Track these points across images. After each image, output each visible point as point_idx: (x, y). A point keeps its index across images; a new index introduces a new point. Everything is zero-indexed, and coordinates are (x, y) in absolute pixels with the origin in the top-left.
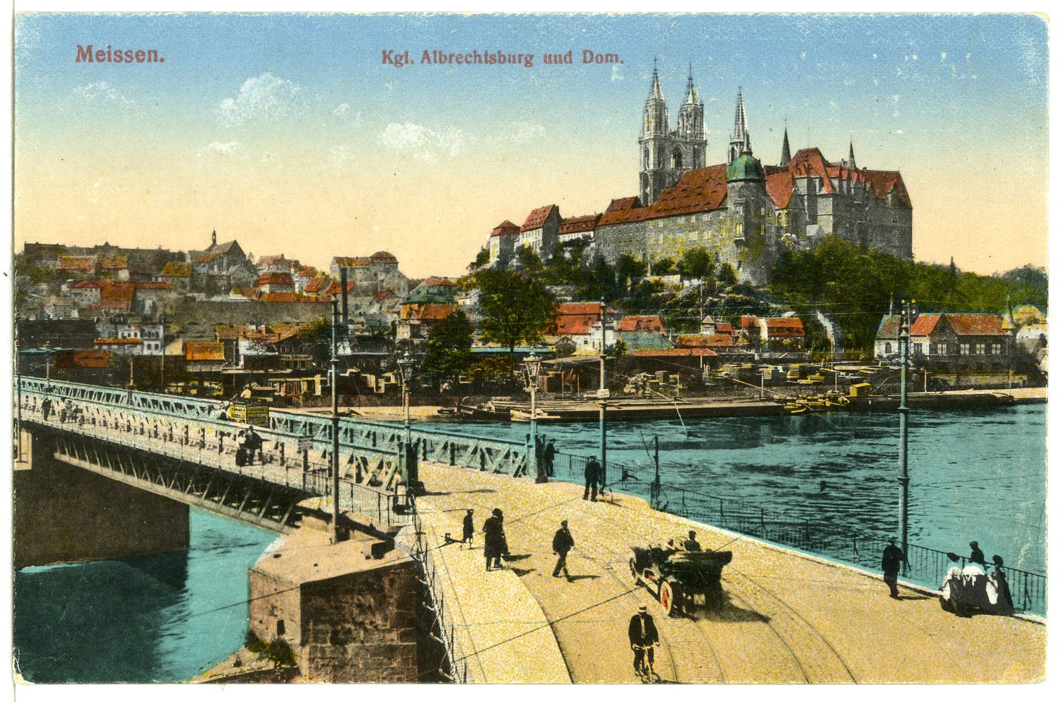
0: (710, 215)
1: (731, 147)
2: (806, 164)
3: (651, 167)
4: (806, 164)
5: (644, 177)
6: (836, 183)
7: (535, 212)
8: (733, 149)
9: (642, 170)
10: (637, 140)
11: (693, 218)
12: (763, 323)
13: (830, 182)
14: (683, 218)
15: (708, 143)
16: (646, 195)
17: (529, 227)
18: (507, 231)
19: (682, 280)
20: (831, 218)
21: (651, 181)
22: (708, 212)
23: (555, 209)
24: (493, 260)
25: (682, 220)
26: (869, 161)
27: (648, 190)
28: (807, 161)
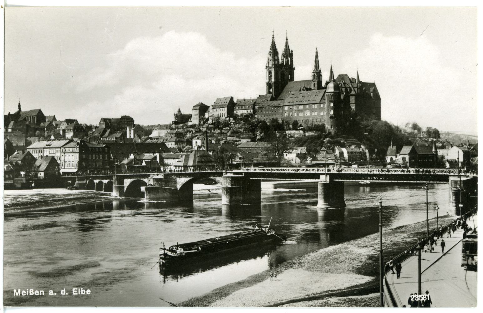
0: (315, 106)
2: (343, 81)
3: (273, 80)
4: (343, 81)
5: (269, 85)
6: (356, 89)
8: (314, 75)
9: (268, 81)
10: (265, 67)
11: (307, 106)
12: (344, 150)
13: (354, 90)
14: (302, 106)
15: (295, 69)
16: (270, 93)
17: (216, 106)
18: (203, 109)
19: (304, 133)
20: (355, 104)
22: (315, 104)
23: (232, 99)
24: (195, 121)
25: (301, 107)
26: (363, 79)
27: (271, 90)
28: (344, 80)
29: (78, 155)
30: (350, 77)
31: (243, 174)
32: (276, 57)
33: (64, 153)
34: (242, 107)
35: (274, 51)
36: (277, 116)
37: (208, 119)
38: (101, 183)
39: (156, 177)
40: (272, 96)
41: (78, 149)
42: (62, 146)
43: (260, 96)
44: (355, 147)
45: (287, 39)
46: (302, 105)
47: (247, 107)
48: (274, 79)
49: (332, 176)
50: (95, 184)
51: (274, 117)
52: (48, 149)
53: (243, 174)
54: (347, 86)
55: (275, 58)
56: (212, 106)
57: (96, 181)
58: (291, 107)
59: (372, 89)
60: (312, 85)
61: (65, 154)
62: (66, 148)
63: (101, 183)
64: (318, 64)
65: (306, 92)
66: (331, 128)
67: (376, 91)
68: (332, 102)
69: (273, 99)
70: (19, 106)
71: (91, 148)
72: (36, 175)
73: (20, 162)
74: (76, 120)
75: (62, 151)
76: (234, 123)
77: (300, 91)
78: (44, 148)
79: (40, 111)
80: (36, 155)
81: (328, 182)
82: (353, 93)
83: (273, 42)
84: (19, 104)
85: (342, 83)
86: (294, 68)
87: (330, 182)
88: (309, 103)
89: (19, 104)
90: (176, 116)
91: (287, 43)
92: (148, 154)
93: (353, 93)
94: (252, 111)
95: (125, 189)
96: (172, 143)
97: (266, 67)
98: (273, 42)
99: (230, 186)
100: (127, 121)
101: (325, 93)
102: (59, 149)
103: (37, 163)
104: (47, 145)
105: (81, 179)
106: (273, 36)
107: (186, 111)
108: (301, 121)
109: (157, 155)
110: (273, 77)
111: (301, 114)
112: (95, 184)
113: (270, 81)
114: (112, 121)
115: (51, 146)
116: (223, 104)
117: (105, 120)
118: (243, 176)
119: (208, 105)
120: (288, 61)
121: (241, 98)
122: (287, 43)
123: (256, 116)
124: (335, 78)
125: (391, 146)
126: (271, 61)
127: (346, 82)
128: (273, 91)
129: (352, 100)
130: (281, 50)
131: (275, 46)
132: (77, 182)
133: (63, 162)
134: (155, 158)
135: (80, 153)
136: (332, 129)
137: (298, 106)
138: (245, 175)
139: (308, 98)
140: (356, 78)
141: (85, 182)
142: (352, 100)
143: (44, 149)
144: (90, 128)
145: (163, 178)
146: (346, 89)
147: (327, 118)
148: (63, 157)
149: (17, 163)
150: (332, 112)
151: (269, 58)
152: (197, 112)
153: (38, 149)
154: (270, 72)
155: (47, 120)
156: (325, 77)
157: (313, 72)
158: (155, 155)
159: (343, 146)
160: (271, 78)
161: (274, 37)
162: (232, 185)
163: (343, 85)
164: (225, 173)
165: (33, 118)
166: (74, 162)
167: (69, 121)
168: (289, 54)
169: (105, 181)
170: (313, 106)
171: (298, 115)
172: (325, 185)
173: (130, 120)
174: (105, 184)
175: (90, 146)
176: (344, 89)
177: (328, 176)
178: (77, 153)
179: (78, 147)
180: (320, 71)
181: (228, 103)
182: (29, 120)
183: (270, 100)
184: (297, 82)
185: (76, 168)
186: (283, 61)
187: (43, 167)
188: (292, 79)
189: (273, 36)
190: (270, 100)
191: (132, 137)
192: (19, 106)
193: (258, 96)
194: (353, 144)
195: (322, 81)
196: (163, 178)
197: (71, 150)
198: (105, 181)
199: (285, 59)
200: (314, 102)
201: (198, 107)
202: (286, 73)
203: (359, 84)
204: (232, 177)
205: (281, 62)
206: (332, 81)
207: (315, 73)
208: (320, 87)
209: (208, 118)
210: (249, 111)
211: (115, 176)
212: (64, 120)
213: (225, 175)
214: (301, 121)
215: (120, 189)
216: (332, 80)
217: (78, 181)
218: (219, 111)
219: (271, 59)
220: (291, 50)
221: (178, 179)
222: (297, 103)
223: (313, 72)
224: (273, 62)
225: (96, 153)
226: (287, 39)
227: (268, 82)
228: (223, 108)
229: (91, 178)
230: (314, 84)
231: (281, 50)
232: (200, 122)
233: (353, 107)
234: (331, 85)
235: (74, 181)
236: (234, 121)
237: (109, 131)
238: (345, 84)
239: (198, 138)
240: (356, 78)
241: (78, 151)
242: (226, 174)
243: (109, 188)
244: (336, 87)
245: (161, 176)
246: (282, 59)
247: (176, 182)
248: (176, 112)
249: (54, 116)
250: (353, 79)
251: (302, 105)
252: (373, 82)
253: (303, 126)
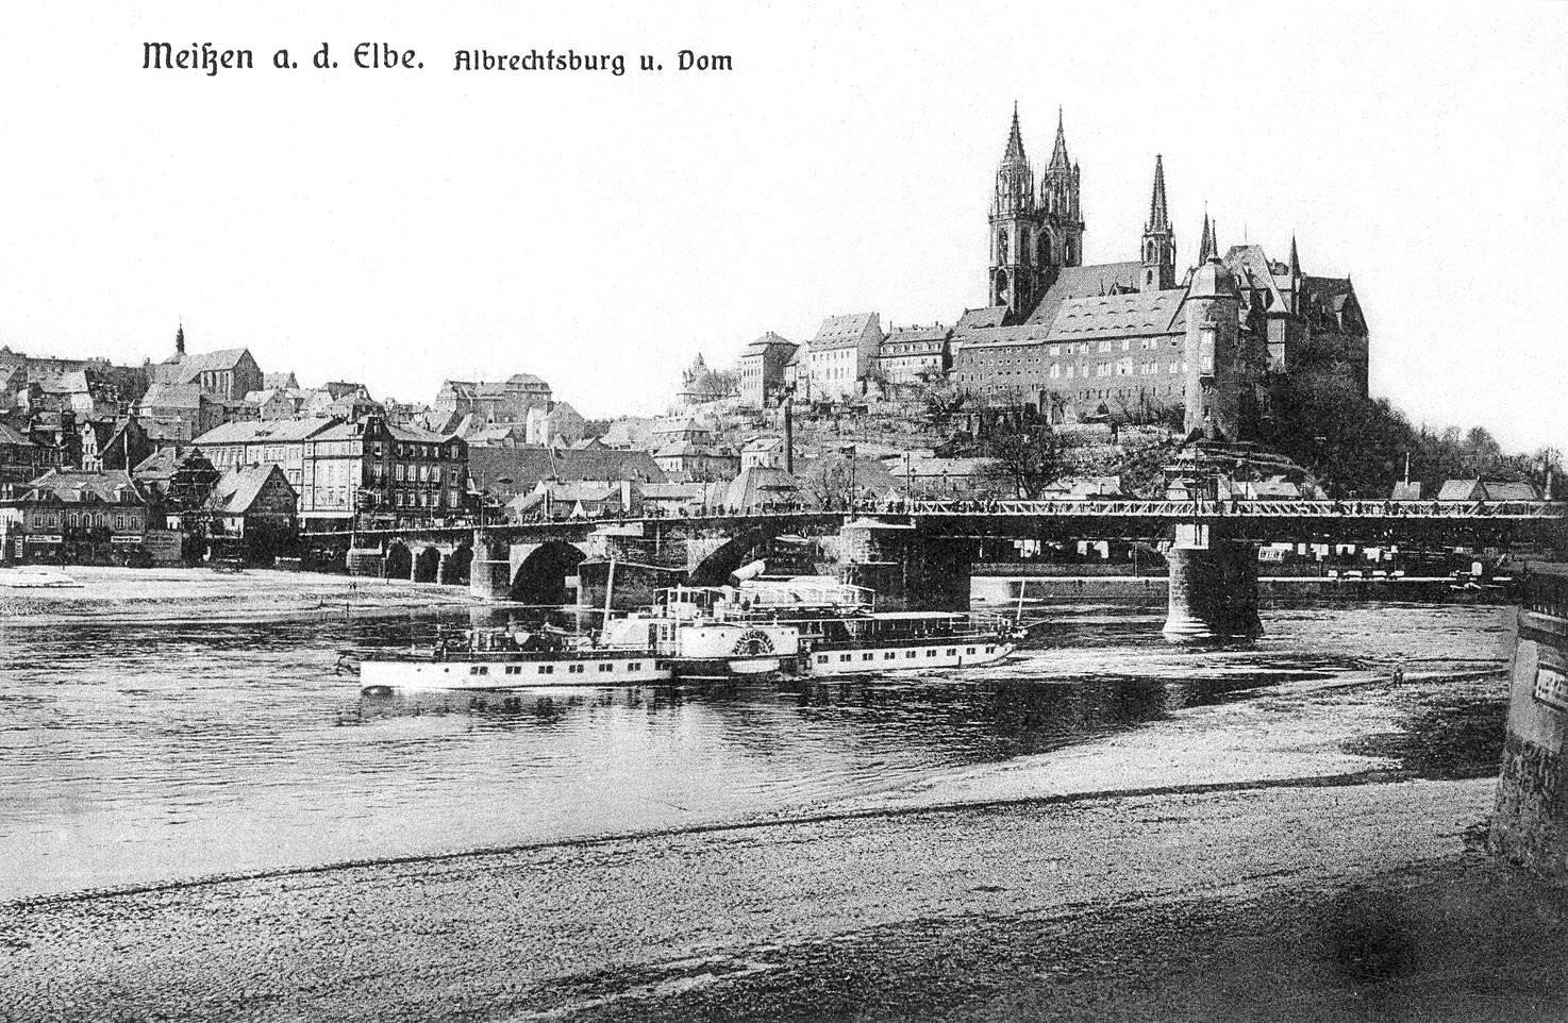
1: (1146, 243)
3: (1011, 261)
4: (1246, 268)
5: (999, 279)
6: (1288, 296)
7: (835, 321)
8: (1150, 244)
9: (995, 263)
11: (1126, 344)
14: (1109, 343)
16: (1001, 302)
18: (778, 355)
21: (1011, 282)
22: (1150, 336)
23: (875, 318)
24: (753, 395)
25: (1105, 347)
27: (1004, 295)
28: (1248, 264)
29: (359, 463)
30: (1271, 261)
31: (913, 521)
32: (1023, 186)
33: (315, 459)
36: (1024, 380)
37: (792, 389)
38: (432, 554)
39: (615, 530)
40: (1009, 308)
41: (360, 445)
42: (308, 437)
43: (967, 312)
44: (1283, 480)
46: (1107, 339)
47: (925, 348)
48: (1016, 257)
49: (1222, 529)
50: (414, 559)
51: (1014, 379)
52: (261, 447)
53: (913, 521)
54: (1258, 286)
55: (1019, 187)
56: (809, 343)
57: (417, 549)
58: (1072, 346)
59: (1339, 301)
60: (1144, 274)
61: (318, 463)
62: (319, 441)
63: (432, 554)
64: (1165, 210)
65: (1119, 297)
66: (1206, 414)
67: (1352, 306)
69: (1009, 320)
71: (404, 442)
72: (218, 528)
73: (166, 485)
74: (363, 387)
75: (306, 451)
76: (879, 399)
77: (1102, 294)
78: (247, 444)
79: (247, 351)
80: (217, 461)
81: (1205, 546)
82: (1278, 306)
83: (1015, 137)
84: (181, 331)
85: (1243, 275)
86: (1083, 224)
87: (1210, 544)
88: (1131, 332)
89: (181, 331)
90: (690, 378)
91: (1060, 141)
92: (595, 485)
93: (1278, 306)
94: (939, 359)
95: (514, 572)
96: (674, 460)
97: (991, 217)
98: (1015, 137)
99: (867, 562)
100: (535, 392)
101: (1185, 299)
102: (301, 446)
103: (224, 487)
104: (258, 434)
105: (371, 541)
106: (1016, 116)
107: (721, 361)
108: (1104, 394)
109: (626, 487)
110: (1011, 252)
111: (1102, 371)
112: (414, 559)
113: (1001, 264)
114: (480, 391)
115: (270, 438)
116: (845, 334)
117: (455, 386)
118: (914, 527)
119: (796, 343)
120: (1063, 199)
121: (907, 323)
122: (1060, 141)
123: (953, 377)
125: (1404, 480)
126: (1007, 200)
127: (1254, 272)
128: (1012, 297)
129: (1276, 330)
130: (1039, 159)
132: (352, 551)
133: (311, 488)
134: (618, 495)
135: (368, 455)
136: (1208, 418)
138: (916, 523)
139: (1130, 319)
140: (1287, 261)
141: (379, 551)
142: (1276, 330)
143: (248, 447)
144: (408, 412)
145: (640, 533)
146: (1255, 295)
147: (1192, 385)
148: (309, 475)
149: (154, 485)
151: (1000, 188)
152: (759, 364)
153: (228, 448)
154: (1003, 236)
155: (266, 385)
156: (1186, 255)
157: (1146, 236)
158: (616, 486)
159: (1244, 475)
160: (1006, 256)
162: (872, 558)
163: (1245, 282)
164: (850, 519)
165: (222, 375)
166: (347, 490)
167: (337, 389)
168: (1065, 177)
169: (447, 550)
170: (1145, 342)
171: (1093, 373)
172: (1190, 554)
173: (539, 389)
174: (447, 557)
175: (399, 436)
176: (1247, 295)
177: (1205, 528)
178: (357, 458)
179: (361, 437)
180: (1170, 233)
181: (861, 331)
182: (210, 382)
183: (1003, 324)
184: (1086, 269)
185: (352, 508)
186: (1047, 205)
187: (239, 504)
188: (1073, 260)
189: (1016, 116)
190: (1003, 324)
191: (544, 440)
193: (961, 313)
194: (1279, 471)
195: (1173, 267)
196: (640, 533)
197: (337, 449)
198: (447, 550)
199: (1052, 194)
200: (1151, 331)
201: (761, 349)
202: (1056, 239)
203: (1298, 282)
204: (873, 530)
205: (1038, 202)
206: (1210, 260)
207: (1152, 239)
208: (1167, 282)
209: (794, 384)
210: (930, 359)
211: (479, 530)
212: (321, 383)
213: (848, 524)
214: (1104, 394)
215: (498, 574)
216: (1212, 256)
217: (356, 546)
218: (832, 358)
219: (1007, 192)
220: (1072, 167)
221: (690, 542)
222: (1089, 335)
223: (1146, 236)
224: (1013, 203)
225: (420, 460)
226: (1060, 130)
227: (996, 269)
228: (845, 351)
229: (398, 539)
230: (1150, 274)
231: (1039, 159)
232: (766, 396)
233: (1278, 355)
234: (1208, 273)
235: (345, 543)
236: (880, 394)
237: (468, 419)
238: (1250, 277)
239: (760, 446)
240: (1287, 261)
241: (358, 448)
242: (854, 521)
243: (458, 571)
244: (1224, 281)
245: (634, 530)
246: (1042, 195)
247: (683, 548)
248: (689, 363)
249: (292, 375)
250: (1277, 264)
251: (1107, 339)
252: (1346, 277)
253: (1110, 409)
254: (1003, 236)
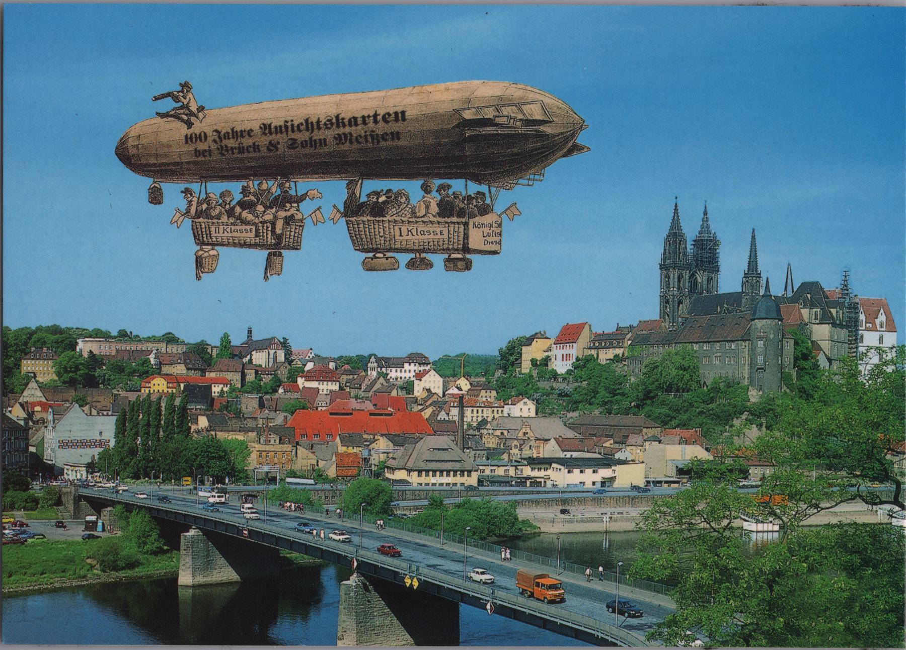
14: (709, 345)
34: (605, 345)
35: (675, 237)
45: (705, 213)
68: (761, 338)
70: (250, 332)
91: (705, 219)
97: (661, 265)
124: (795, 290)
130: (691, 231)
131: (679, 228)
137: (702, 344)
150: (760, 359)
157: (745, 277)
161: (678, 208)
192: (250, 332)
226: (705, 213)
254: (668, 277)
